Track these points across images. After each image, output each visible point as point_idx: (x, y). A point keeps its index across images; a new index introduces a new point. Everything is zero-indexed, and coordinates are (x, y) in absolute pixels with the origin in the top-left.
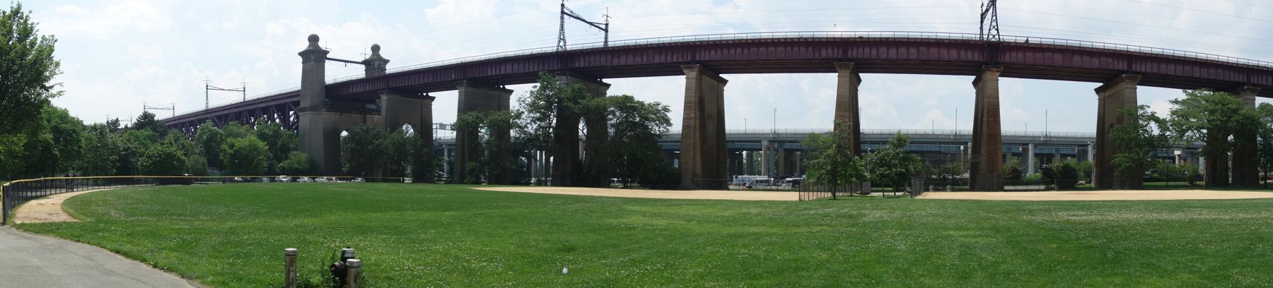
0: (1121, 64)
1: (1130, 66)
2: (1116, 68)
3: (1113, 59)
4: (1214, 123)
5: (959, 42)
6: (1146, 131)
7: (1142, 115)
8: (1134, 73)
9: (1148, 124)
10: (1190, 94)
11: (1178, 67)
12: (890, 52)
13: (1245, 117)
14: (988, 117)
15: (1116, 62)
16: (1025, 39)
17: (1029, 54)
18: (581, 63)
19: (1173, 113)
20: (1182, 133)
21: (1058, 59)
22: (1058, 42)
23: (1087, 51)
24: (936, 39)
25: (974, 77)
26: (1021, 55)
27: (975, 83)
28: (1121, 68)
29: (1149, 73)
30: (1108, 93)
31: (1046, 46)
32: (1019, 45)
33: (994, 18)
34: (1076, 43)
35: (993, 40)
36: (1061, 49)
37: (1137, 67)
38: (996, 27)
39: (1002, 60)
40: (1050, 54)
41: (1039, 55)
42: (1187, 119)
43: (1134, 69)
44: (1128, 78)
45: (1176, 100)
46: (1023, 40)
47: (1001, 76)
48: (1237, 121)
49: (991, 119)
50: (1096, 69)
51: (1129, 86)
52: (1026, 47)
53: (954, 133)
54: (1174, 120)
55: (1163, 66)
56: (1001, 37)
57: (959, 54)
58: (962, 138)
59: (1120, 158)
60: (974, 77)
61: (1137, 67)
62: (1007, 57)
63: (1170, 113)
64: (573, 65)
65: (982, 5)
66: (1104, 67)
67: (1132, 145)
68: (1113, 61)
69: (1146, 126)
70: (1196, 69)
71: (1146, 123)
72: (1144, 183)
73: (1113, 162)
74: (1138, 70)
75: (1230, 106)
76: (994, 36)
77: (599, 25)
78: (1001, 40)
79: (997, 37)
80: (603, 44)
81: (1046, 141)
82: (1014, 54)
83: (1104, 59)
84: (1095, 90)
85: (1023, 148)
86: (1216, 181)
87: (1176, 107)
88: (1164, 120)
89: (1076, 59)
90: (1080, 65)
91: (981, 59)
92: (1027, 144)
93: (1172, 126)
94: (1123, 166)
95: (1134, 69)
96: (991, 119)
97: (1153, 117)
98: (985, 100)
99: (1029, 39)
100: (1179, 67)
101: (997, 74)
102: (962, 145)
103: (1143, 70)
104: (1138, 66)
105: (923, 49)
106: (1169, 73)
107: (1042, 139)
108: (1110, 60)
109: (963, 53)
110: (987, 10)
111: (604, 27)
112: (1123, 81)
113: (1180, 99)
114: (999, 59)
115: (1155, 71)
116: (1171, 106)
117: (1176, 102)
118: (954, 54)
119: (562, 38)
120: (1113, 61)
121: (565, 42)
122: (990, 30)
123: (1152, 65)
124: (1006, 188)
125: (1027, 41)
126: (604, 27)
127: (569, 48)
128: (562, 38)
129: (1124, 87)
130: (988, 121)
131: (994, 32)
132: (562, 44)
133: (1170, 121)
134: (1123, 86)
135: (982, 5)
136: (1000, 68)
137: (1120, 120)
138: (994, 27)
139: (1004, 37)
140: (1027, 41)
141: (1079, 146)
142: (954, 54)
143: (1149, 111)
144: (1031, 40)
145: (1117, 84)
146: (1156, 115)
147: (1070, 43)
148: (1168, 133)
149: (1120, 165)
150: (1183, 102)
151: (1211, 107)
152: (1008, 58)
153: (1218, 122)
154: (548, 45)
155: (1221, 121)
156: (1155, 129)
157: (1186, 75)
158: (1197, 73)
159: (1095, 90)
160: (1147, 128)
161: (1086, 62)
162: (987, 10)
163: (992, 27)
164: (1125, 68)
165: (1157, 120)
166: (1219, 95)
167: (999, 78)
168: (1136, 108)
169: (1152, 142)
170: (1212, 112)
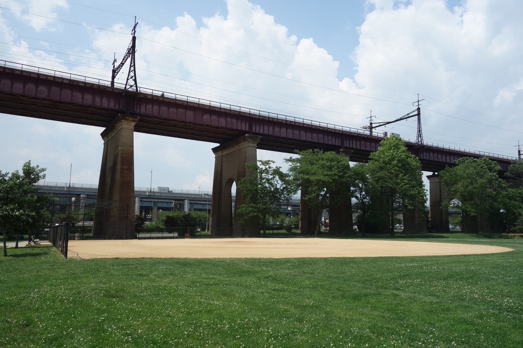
0: (243, 125)
1: (251, 127)
2: (239, 128)
5: (95, 87)
11: (288, 130)
12: (14, 86)
15: (239, 123)
16: (161, 93)
17: (164, 108)
24: (70, 80)
26: (156, 108)
31: (180, 103)
32: (155, 98)
33: (132, 68)
39: (138, 111)
40: (183, 111)
41: (173, 110)
43: (254, 131)
44: (250, 137)
46: (159, 94)
51: (251, 144)
55: (277, 129)
56: (138, 89)
66: (229, 126)
70: (303, 133)
74: (257, 131)
76: (131, 86)
78: (139, 91)
79: (135, 88)
82: (149, 107)
83: (229, 119)
89: (206, 117)
90: (209, 123)
91: (117, 107)
95: (254, 131)
98: (120, 148)
99: (165, 94)
104: (258, 128)
105: (54, 89)
106: (282, 136)
108: (234, 121)
109: (98, 100)
112: (245, 140)
114: (135, 110)
115: (271, 133)
122: (128, 79)
123: (269, 128)
125: (163, 95)
129: (247, 145)
131: (131, 82)
139: (141, 89)
140: (163, 95)
142: (88, 99)
144: (166, 95)
152: (144, 109)
157: (295, 138)
161: (214, 121)
163: (130, 77)
164: (247, 129)
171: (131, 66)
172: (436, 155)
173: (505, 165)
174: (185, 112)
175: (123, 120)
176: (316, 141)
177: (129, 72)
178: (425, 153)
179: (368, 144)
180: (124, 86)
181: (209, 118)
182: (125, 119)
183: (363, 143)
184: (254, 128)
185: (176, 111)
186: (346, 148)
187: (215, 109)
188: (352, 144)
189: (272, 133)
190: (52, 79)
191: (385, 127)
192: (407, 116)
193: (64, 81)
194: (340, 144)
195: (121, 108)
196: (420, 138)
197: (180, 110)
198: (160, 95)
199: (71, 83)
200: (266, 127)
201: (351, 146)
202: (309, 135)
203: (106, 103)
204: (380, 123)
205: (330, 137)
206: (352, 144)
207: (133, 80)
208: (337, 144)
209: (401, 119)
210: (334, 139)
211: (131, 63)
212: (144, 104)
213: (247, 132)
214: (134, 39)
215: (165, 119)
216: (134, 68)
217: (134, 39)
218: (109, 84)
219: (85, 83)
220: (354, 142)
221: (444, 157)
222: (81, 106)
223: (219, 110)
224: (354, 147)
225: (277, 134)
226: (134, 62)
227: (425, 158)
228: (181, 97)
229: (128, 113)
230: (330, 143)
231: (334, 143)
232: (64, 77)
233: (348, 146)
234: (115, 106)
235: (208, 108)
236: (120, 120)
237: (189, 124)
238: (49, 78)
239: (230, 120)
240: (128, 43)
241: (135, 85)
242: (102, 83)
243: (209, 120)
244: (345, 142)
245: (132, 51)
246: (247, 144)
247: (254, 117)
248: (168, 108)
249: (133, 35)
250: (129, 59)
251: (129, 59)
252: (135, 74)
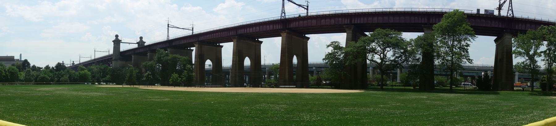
18: (293, 25)
33: (510, 5)
35: (510, 16)
64: (290, 27)
77: (304, 6)
79: (512, 15)
80: (306, 14)
111: (306, 7)
119: (283, 12)
121: (285, 13)
122: (508, 11)
126: (306, 7)
127: (287, 17)
128: (283, 12)
131: (510, 12)
132: (283, 15)
154: (275, 15)
163: (509, 10)
171: (510, 4)
177: (509, 7)
211: (510, 2)
216: (512, 5)
226: (511, 2)
252: (512, 8)
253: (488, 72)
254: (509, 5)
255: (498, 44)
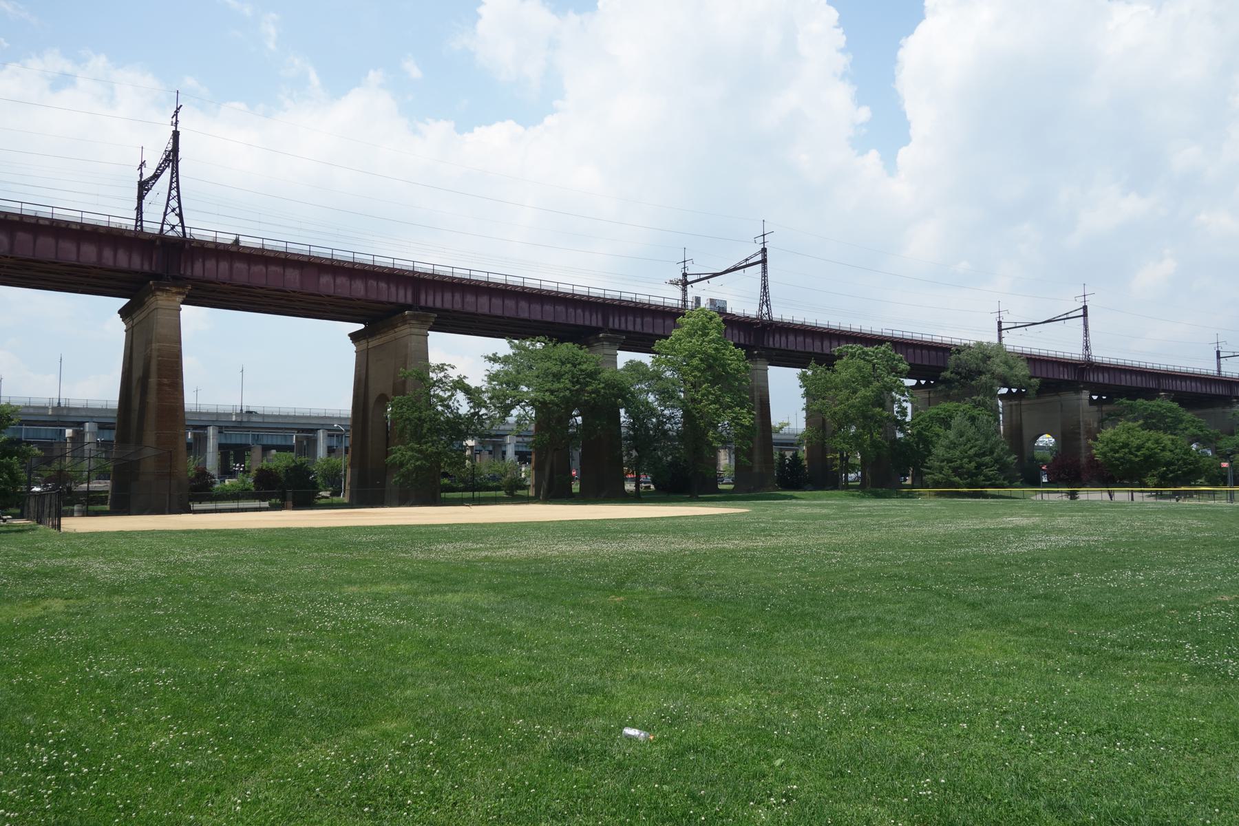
0: (401, 292)
1: (416, 297)
2: (393, 299)
3: (388, 284)
4: (562, 394)
5: (102, 231)
6: (448, 407)
7: (440, 380)
8: (422, 308)
9: (453, 395)
10: (517, 347)
11: (493, 300)
13: (610, 385)
14: (160, 376)
15: (393, 289)
16: (234, 237)
17: (240, 266)
19: (492, 377)
20: (506, 410)
21: (293, 278)
22: (294, 248)
23: (343, 268)
24: (52, 221)
25: (123, 302)
26: (224, 266)
27: (124, 313)
28: (401, 300)
29: (447, 311)
30: (373, 343)
31: (272, 255)
32: (221, 247)
33: (174, 193)
34: (325, 253)
35: (171, 234)
36: (298, 261)
37: (428, 299)
38: (177, 210)
39: (189, 273)
40: (279, 270)
41: (258, 269)
42: (516, 387)
43: (423, 303)
45: (494, 355)
46: (228, 239)
47: (184, 303)
48: (596, 391)
49: (165, 381)
50: (359, 300)
51: (416, 331)
52: (233, 253)
53: (55, 405)
54: (494, 389)
55: (470, 299)
56: (187, 230)
57: (100, 255)
58: (73, 413)
59: (401, 453)
60: (123, 302)
61: (428, 299)
62: (198, 267)
63: (486, 379)
65: (143, 164)
66: (373, 296)
67: (425, 431)
68: (389, 288)
69: (450, 397)
70: (523, 304)
71: (449, 394)
72: (443, 495)
73: (391, 457)
74: (430, 304)
75: (584, 367)
76: (173, 227)
78: (188, 236)
79: (179, 229)
81: (241, 422)
82: (210, 264)
83: (373, 283)
84: (350, 335)
85: (194, 435)
86: (556, 492)
87: (497, 367)
88: (478, 390)
89: (325, 279)
90: (331, 292)
91: (146, 268)
92: (205, 427)
93: (490, 399)
94: (410, 466)
95: (423, 303)
96: (165, 381)
97: (460, 385)
98: (155, 346)
99: (241, 238)
100: (497, 302)
101: (179, 298)
102: (69, 427)
103: (438, 304)
105: (22, 236)
106: (480, 311)
107: (234, 419)
108: (383, 285)
109: (108, 254)
110: (156, 177)
112: (404, 321)
113: (500, 355)
114: (182, 272)
115: (458, 306)
116: (489, 365)
117: (494, 359)
118: (89, 253)
120: (389, 288)
122: (165, 214)
123: (453, 296)
124: (197, 506)
125: (237, 241)
130: (160, 384)
131: (173, 219)
133: (487, 391)
134: (404, 331)
135: (143, 164)
136: (184, 287)
137: (400, 388)
138: (173, 210)
139: (193, 231)
140: (237, 241)
141: (299, 430)
142: (89, 253)
143: (454, 375)
144: (245, 241)
145: (394, 327)
146: (466, 381)
147: (316, 252)
148: (483, 411)
149: (402, 465)
150: (506, 360)
151: (555, 369)
153: (567, 393)
155: (571, 391)
156: (463, 405)
157: (507, 314)
158: (524, 311)
159: (350, 335)
160: (451, 403)
161: (342, 286)
162: (156, 177)
163: (169, 210)
164: (410, 300)
165: (467, 390)
166: (566, 349)
167: (182, 306)
168: (428, 367)
169: (458, 427)
170: (557, 377)
171: (170, 189)
172: (800, 339)
173: (941, 354)
174: (282, 272)
175: (158, 293)
176: (550, 319)
177: (169, 200)
178: (777, 337)
179: (659, 321)
180: (159, 226)
181: (332, 281)
182: (163, 291)
183: (648, 319)
184: (423, 297)
185: (264, 270)
186: (613, 331)
187: (342, 264)
188: (626, 323)
189: (460, 306)
190: (17, 218)
191: (692, 286)
192: (745, 264)
193: (41, 222)
194: (600, 324)
195: (154, 269)
196: (765, 307)
197: (273, 268)
198: (230, 242)
199: (54, 224)
200: (448, 296)
201: (623, 326)
202: (536, 308)
203: (122, 260)
204: (700, 274)
205: (579, 311)
206: (626, 323)
207: (176, 215)
208: (594, 324)
209: (735, 269)
210: (587, 314)
211: (171, 183)
212: (200, 260)
213: (409, 307)
214: (176, 135)
215: (243, 286)
216: (178, 192)
217: (176, 135)
218: (130, 224)
219: (82, 225)
220: (630, 318)
221: (818, 343)
222: (74, 266)
223: (350, 266)
224: (630, 328)
225: (471, 309)
226: (177, 181)
227: (777, 346)
228: (274, 243)
229: (169, 277)
230: (580, 322)
231: (587, 323)
232: (40, 215)
233: (617, 326)
234: (142, 265)
235: (328, 263)
236: (153, 293)
237: (292, 294)
238: (10, 218)
239: (375, 283)
240: (166, 143)
241: (180, 224)
242: (115, 222)
243: (332, 285)
244: (611, 320)
245: (172, 158)
246: (408, 330)
247: (421, 276)
248: (249, 265)
249: (174, 128)
250: (168, 171)
251: (168, 171)
252: (179, 203)
253: (87, 424)
254: (170, 193)
255: (133, 327)
